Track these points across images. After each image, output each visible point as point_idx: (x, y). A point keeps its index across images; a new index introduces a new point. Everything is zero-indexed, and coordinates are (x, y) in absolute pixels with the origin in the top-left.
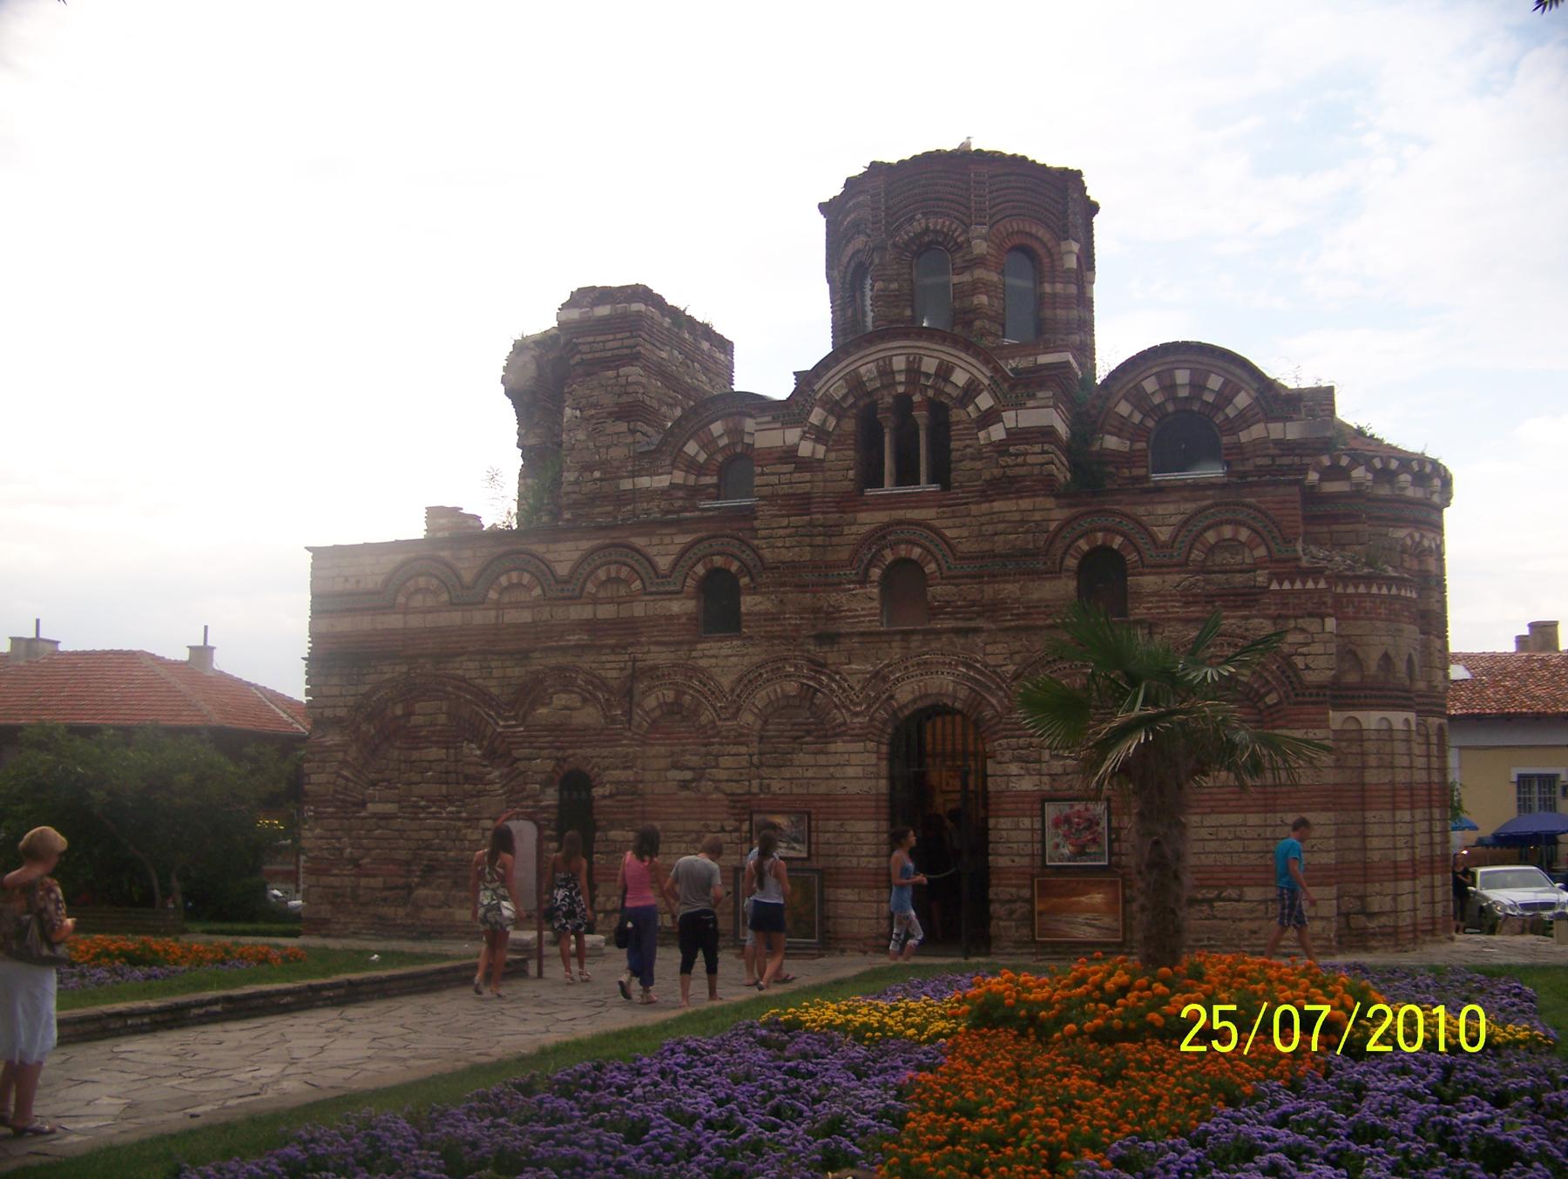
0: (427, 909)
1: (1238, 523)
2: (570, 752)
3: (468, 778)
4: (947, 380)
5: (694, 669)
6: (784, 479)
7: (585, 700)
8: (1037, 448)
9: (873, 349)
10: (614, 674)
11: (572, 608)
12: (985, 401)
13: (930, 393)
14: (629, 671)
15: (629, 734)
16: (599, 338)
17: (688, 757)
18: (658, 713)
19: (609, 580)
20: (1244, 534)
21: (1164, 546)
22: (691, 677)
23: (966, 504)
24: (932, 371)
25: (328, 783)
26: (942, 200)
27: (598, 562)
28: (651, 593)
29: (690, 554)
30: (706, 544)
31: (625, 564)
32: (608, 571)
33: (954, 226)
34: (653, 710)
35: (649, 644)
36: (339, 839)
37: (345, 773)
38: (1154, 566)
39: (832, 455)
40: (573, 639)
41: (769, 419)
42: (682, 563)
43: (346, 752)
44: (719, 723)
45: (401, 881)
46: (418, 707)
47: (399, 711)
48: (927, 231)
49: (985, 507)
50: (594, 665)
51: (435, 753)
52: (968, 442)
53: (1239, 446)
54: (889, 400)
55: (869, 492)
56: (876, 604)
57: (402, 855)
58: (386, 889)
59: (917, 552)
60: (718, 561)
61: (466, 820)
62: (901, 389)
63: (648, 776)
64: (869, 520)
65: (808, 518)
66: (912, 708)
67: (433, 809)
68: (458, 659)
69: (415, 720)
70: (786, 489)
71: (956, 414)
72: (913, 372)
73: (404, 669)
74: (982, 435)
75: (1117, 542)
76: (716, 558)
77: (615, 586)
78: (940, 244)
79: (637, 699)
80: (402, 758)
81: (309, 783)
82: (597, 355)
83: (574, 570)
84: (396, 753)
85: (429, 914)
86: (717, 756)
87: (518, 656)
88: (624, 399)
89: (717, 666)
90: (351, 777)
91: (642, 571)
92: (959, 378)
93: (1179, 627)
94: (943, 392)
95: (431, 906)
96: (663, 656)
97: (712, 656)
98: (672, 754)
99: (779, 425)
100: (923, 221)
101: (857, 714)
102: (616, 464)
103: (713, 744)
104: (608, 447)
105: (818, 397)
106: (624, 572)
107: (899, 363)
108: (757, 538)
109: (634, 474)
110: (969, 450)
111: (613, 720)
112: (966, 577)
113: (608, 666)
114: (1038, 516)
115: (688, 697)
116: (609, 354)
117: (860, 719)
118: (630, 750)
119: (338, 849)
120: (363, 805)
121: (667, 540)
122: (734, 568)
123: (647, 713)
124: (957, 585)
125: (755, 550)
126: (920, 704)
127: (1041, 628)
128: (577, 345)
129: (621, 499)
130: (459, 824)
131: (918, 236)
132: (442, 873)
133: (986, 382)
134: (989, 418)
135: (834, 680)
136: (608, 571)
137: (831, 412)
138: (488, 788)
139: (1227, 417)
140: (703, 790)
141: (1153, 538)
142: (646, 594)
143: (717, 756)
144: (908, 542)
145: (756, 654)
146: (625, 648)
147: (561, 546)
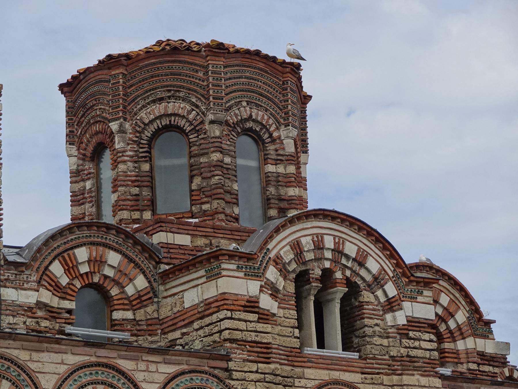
4: (361, 264)
6: (251, 326)
8: (426, 336)
9: (309, 224)
12: (391, 290)
13: (348, 273)
23: (378, 373)
24: (354, 256)
26: (261, 95)
27: (84, 380)
30: (187, 377)
33: (271, 122)
39: (281, 313)
41: (234, 267)
52: (376, 321)
53: (457, 352)
62: (327, 264)
65: (272, 366)
70: (253, 337)
71: (366, 296)
72: (338, 251)
74: (389, 317)
92: (373, 265)
94: (358, 275)
99: (242, 275)
100: (248, 109)
105: (272, 255)
107: (329, 242)
110: (377, 329)
133: (391, 275)
137: (280, 271)
139: (448, 327)
147: (45, 356)
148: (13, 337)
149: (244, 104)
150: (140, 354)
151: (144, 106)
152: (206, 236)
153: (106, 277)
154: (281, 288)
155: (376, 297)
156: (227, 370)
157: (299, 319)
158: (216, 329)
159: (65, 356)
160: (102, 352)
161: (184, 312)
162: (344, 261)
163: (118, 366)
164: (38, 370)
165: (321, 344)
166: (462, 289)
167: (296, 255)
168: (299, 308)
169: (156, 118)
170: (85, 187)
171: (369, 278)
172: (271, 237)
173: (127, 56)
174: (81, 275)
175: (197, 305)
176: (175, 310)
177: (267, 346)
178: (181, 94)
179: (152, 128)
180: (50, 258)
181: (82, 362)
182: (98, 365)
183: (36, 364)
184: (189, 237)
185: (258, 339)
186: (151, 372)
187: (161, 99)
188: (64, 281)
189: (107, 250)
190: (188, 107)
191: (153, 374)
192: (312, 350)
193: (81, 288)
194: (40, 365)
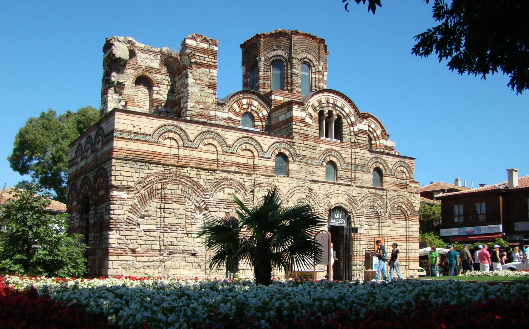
0: (172, 270)
1: (404, 167)
2: (231, 210)
3: (187, 217)
4: (343, 110)
7: (235, 192)
8: (365, 136)
13: (338, 112)
16: (202, 55)
19: (246, 150)
20: (405, 170)
21: (390, 170)
25: (124, 214)
26: (311, 49)
29: (273, 146)
31: (252, 145)
38: (389, 175)
39: (313, 124)
40: (233, 169)
41: (297, 107)
42: (270, 149)
46: (169, 186)
47: (160, 187)
48: (306, 58)
49: (353, 150)
50: (240, 180)
51: (175, 205)
54: (326, 111)
55: (322, 138)
56: (325, 173)
58: (149, 261)
59: (335, 160)
60: (283, 151)
61: (185, 234)
62: (330, 109)
64: (324, 147)
65: (309, 142)
66: (334, 206)
68: (186, 169)
69: (167, 191)
70: (301, 131)
71: (344, 121)
72: (335, 105)
73: (163, 169)
74: (351, 128)
75: (381, 167)
77: (247, 152)
78: (308, 63)
81: (114, 214)
82: (202, 61)
87: (212, 172)
88: (212, 81)
91: (257, 148)
93: (392, 192)
96: (265, 180)
99: (300, 110)
101: (321, 207)
102: (208, 104)
105: (311, 104)
107: (331, 101)
108: (294, 145)
109: (215, 110)
110: (347, 132)
112: (345, 169)
113: (245, 180)
114: (365, 155)
116: (206, 62)
117: (322, 208)
121: (266, 139)
122: (287, 153)
124: (345, 171)
125: (293, 148)
126: (336, 205)
127: (365, 187)
128: (194, 55)
129: (209, 117)
130: (183, 235)
131: (304, 58)
134: (352, 124)
135: (315, 195)
138: (196, 221)
139: (374, 136)
141: (388, 168)
144: (333, 156)
145: (294, 183)
146: (249, 174)
149: (304, 52)
151: (269, 52)
152: (289, 98)
153: (252, 110)
154: (313, 116)
155: (347, 121)
156: (293, 142)
157: (319, 127)
158: (289, 128)
160: (248, 133)
161: (280, 122)
162: (336, 108)
165: (327, 136)
166: (379, 123)
167: (319, 105)
168: (320, 123)
169: (273, 57)
170: (247, 81)
171: (345, 114)
172: (311, 98)
173: (264, 35)
174: (244, 109)
175: (284, 121)
176: (276, 122)
177: (307, 135)
178: (282, 48)
179: (271, 60)
180: (233, 102)
182: (247, 137)
184: (282, 98)
185: (304, 133)
187: (275, 50)
188: (238, 110)
189: (253, 101)
190: (284, 53)
192: (324, 138)
193: (244, 113)
194: (227, 136)
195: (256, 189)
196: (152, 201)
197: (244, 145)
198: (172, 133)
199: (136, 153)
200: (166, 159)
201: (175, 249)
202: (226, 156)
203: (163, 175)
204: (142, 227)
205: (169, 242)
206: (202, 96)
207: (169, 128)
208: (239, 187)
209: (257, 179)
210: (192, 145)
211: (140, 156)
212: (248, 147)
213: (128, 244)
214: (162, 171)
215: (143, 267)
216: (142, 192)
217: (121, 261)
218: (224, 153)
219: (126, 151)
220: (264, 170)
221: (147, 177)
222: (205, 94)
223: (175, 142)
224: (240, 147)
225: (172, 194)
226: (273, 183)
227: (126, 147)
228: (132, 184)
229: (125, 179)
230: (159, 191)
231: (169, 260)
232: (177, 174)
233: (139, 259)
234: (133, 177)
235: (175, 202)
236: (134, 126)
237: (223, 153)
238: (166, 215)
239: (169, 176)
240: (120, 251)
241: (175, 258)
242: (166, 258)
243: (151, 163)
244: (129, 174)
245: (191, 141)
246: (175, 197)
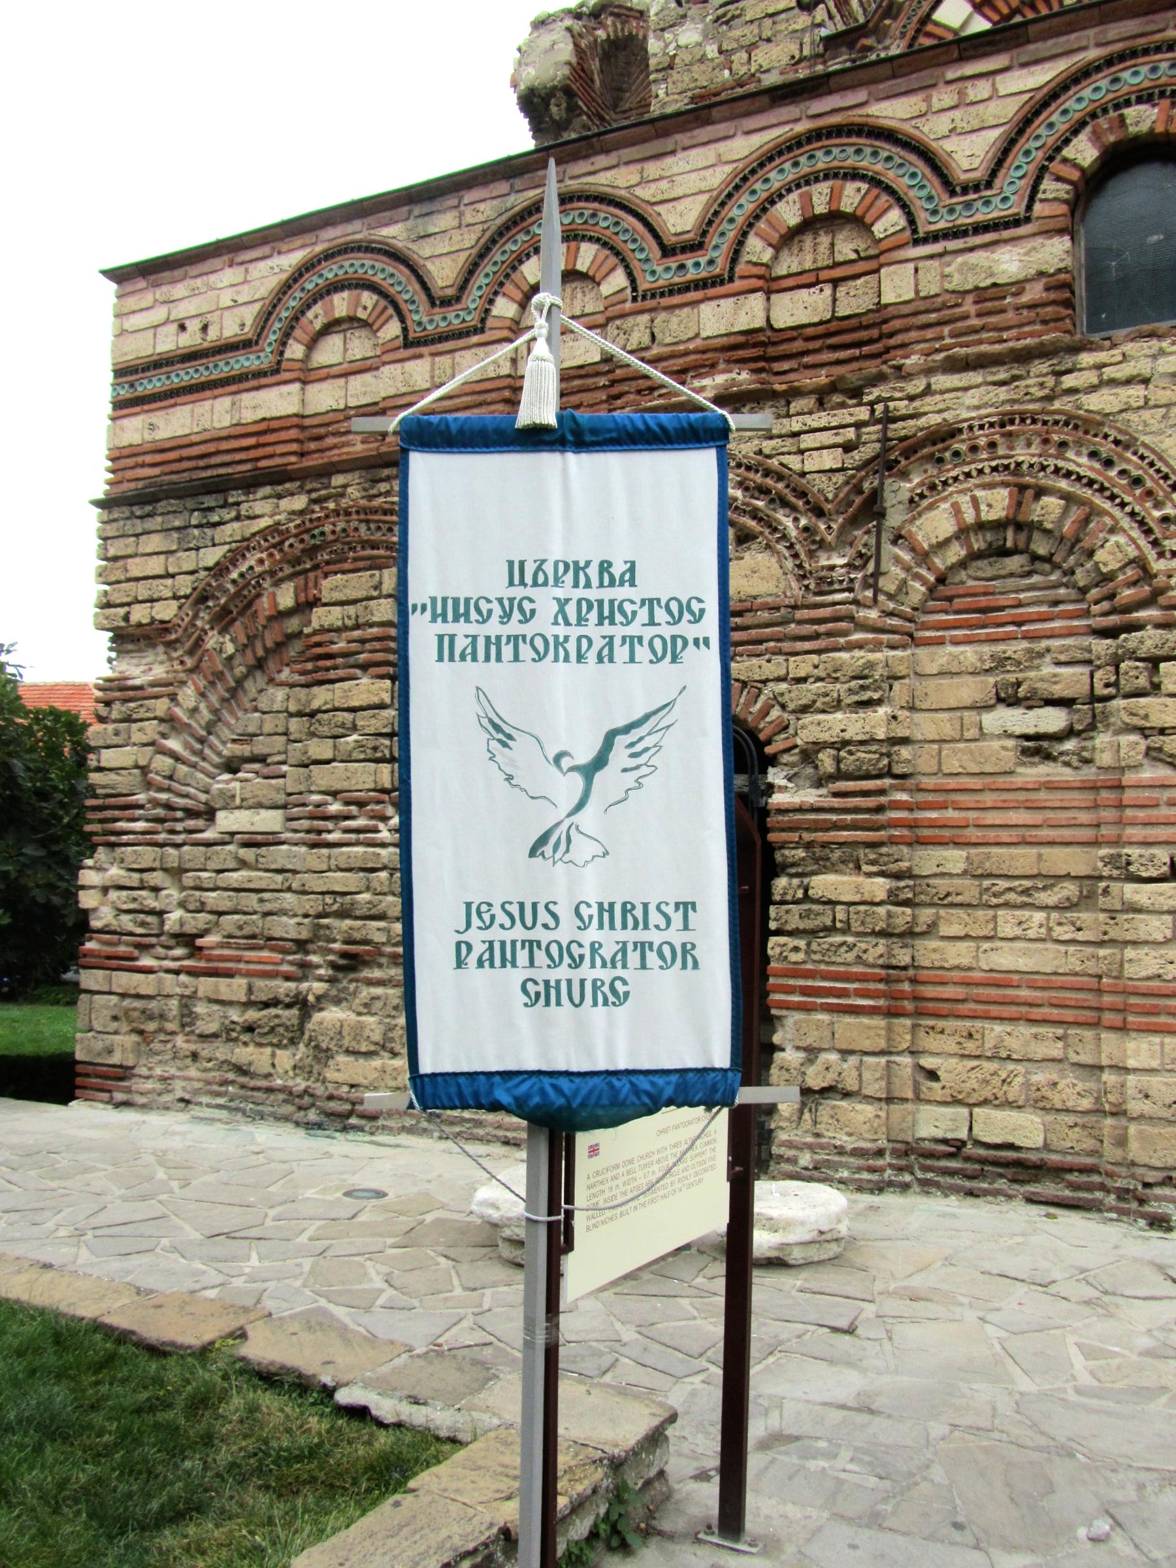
0: (341, 1059)
5: (1070, 421)
10: (829, 459)
11: (706, 309)
14: (867, 451)
15: (873, 614)
17: (1048, 669)
18: (956, 552)
19: (810, 224)
22: (1063, 445)
28: (935, 237)
30: (1102, 81)
31: (854, 175)
32: (807, 201)
34: (944, 544)
35: (929, 371)
36: (156, 890)
37: (173, 744)
43: (173, 697)
44: (1158, 566)
45: (284, 988)
46: (331, 586)
47: (286, 597)
50: (768, 446)
57: (288, 927)
58: (248, 1004)
63: (925, 726)
67: (361, 822)
69: (321, 617)
73: (299, 502)
76: (1130, 113)
77: (824, 240)
79: (895, 518)
80: (293, 708)
81: (100, 769)
83: (708, 223)
84: (280, 694)
85: (343, 1069)
86: (1154, 662)
89: (1146, 405)
90: (186, 754)
91: (902, 183)
95: (348, 1052)
96: (971, 398)
97: (1128, 382)
98: (1001, 662)
103: (1137, 627)
104: (750, 48)
106: (851, 196)
111: (825, 584)
113: (807, 441)
115: (1052, 503)
118: (878, 656)
119: (152, 912)
120: (209, 814)
123: (923, 557)
132: (377, 974)
136: (807, 201)
140: (1105, 758)
142: (916, 242)
143: (1154, 662)
146: (856, 393)
147: (674, 164)
148: (597, 146)
150: (937, 71)
159: (722, 147)
163: (870, 121)
164: (659, 198)
181: (771, 145)
182: (815, 135)
183: (653, 186)
186: (973, 103)
191: (981, 107)
194: (664, 185)
195: (898, 491)
196: (271, 681)
197: (794, 196)
198: (345, 294)
199: (186, 452)
200: (330, 441)
201: (357, 936)
202: (662, 317)
203: (303, 530)
204: (226, 821)
205: (329, 899)
206: (733, 51)
207: (331, 271)
208: (760, 504)
209: (902, 407)
210: (454, 318)
211: (201, 463)
212: (820, 197)
213: (160, 914)
214: (302, 513)
215: (227, 1034)
216: (212, 640)
217: (123, 996)
218: (649, 303)
219: (148, 459)
220: (975, 322)
221: (234, 562)
222: (747, 30)
223: (364, 333)
224: (762, 225)
225: (346, 628)
226: (1057, 405)
227: (148, 437)
228: (166, 611)
229: (142, 589)
230: (293, 624)
231: (337, 1001)
232: (375, 511)
233: (205, 985)
234: (173, 576)
235: (364, 667)
236: (182, 328)
237: (639, 304)
238: (320, 749)
239: (328, 528)
240: (122, 949)
241: (366, 992)
242: (319, 987)
243: (250, 484)
244: (155, 566)
245: (446, 302)
246: (363, 641)
